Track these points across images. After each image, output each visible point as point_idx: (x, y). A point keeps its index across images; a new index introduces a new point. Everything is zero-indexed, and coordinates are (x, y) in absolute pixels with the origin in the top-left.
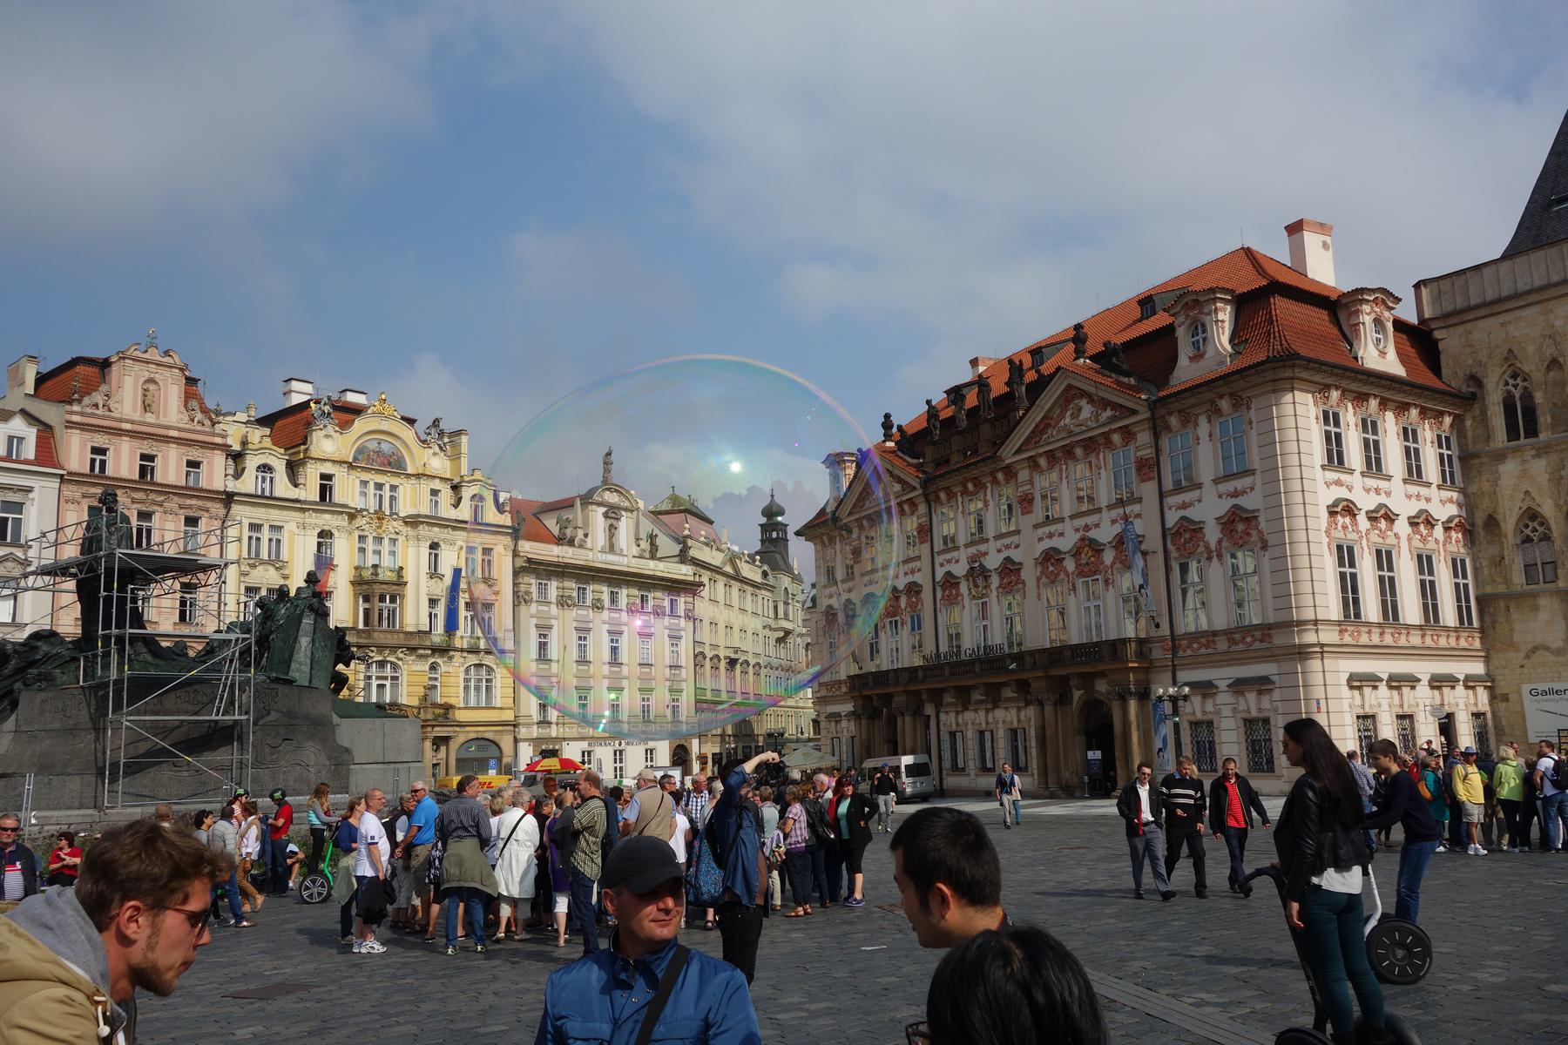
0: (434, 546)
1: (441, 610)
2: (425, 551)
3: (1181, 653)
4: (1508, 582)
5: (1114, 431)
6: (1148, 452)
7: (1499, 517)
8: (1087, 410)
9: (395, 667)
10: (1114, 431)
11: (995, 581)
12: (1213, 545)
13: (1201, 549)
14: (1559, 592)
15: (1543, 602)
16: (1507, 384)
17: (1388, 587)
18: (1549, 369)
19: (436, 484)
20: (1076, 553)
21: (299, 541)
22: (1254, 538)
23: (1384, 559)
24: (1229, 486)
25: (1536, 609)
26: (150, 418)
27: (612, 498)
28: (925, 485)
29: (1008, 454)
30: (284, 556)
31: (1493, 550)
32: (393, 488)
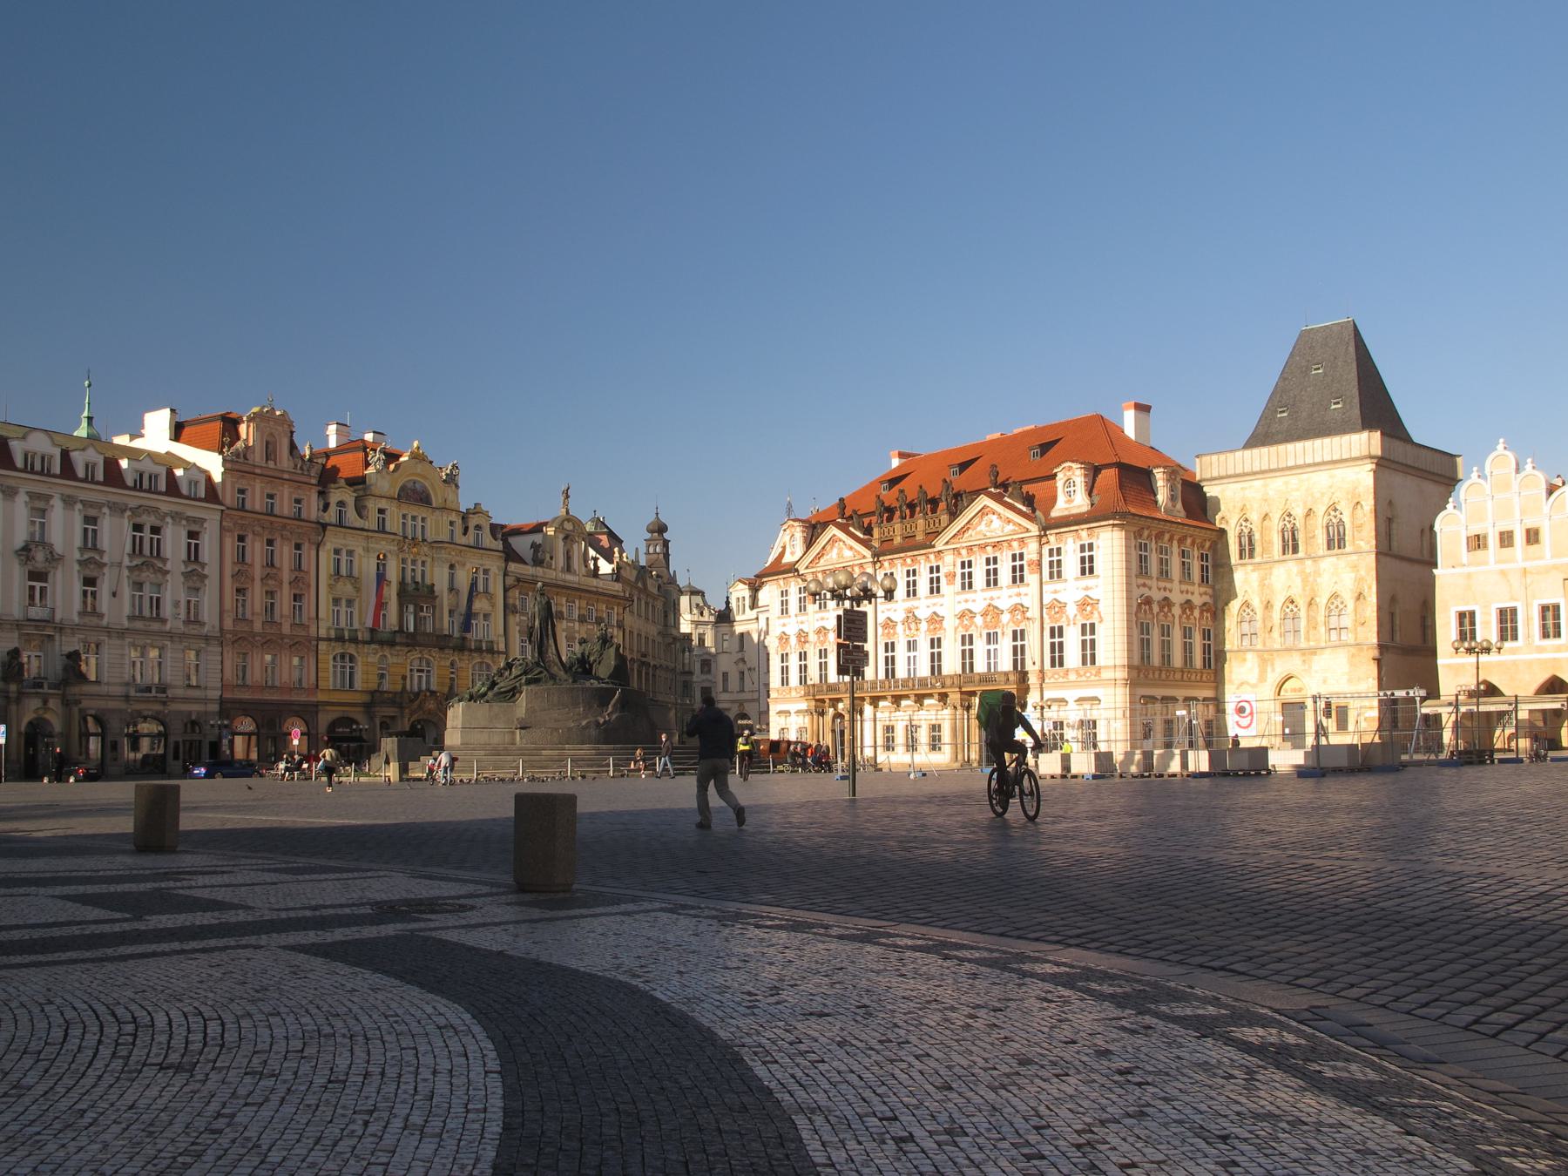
0: (452, 567)
1: (458, 620)
2: (446, 570)
9: (428, 664)
11: (924, 626)
17: (1166, 646)
19: (453, 517)
20: (984, 614)
21: (365, 560)
23: (1166, 631)
26: (271, 464)
27: (568, 526)
28: (874, 555)
30: (356, 573)
32: (423, 520)
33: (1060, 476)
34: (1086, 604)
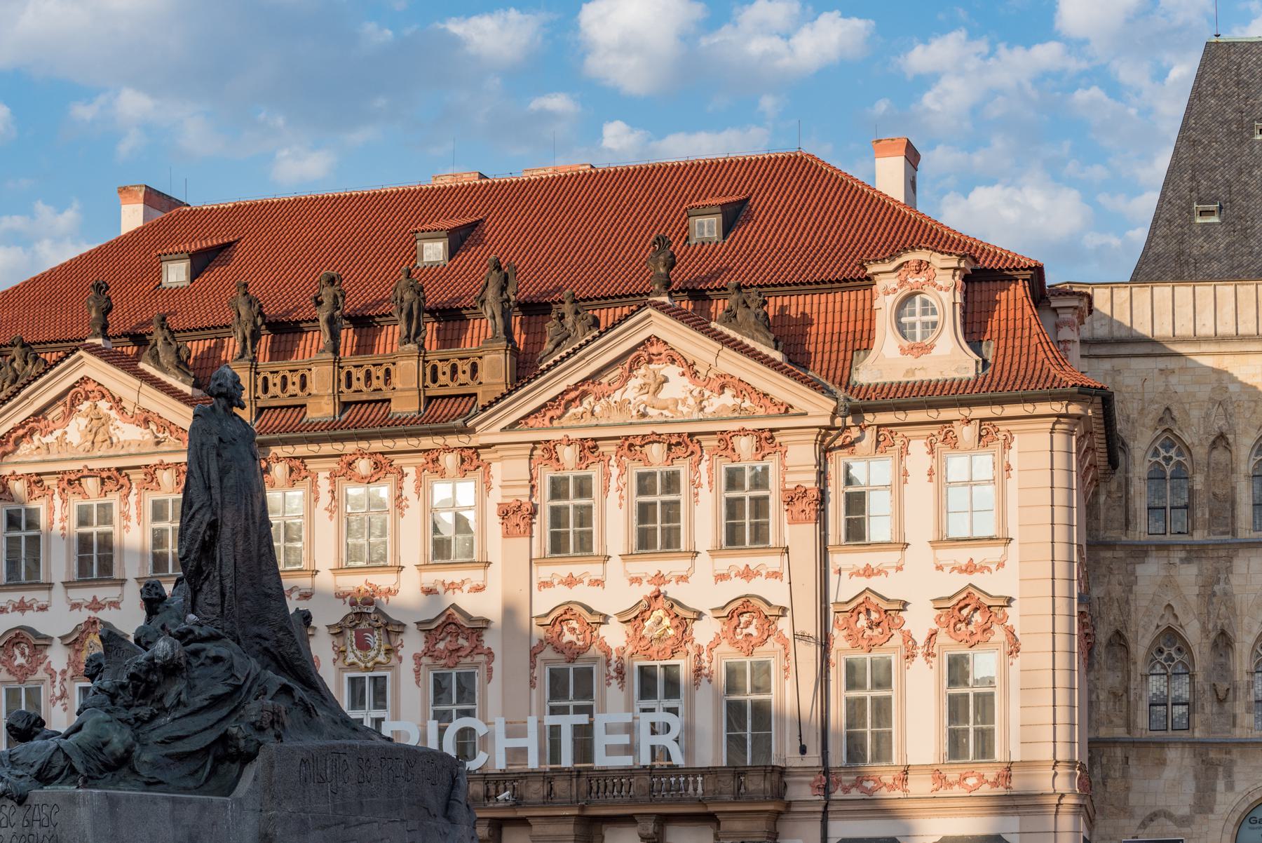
3: (838, 794)
4: (1129, 724)
5: (744, 432)
6: (809, 480)
7: (1129, 636)
8: (678, 386)
10: (744, 432)
11: (412, 643)
12: (921, 638)
13: (897, 639)
14: (1193, 744)
15: (1172, 754)
16: (1156, 453)
18: (1214, 446)
22: (999, 634)
24: (962, 555)
25: (1162, 763)
29: (489, 431)
31: (1112, 679)
33: (882, 283)
34: (968, 611)
